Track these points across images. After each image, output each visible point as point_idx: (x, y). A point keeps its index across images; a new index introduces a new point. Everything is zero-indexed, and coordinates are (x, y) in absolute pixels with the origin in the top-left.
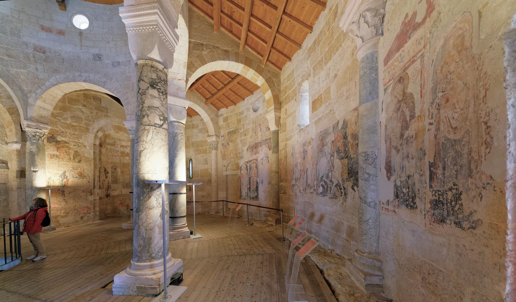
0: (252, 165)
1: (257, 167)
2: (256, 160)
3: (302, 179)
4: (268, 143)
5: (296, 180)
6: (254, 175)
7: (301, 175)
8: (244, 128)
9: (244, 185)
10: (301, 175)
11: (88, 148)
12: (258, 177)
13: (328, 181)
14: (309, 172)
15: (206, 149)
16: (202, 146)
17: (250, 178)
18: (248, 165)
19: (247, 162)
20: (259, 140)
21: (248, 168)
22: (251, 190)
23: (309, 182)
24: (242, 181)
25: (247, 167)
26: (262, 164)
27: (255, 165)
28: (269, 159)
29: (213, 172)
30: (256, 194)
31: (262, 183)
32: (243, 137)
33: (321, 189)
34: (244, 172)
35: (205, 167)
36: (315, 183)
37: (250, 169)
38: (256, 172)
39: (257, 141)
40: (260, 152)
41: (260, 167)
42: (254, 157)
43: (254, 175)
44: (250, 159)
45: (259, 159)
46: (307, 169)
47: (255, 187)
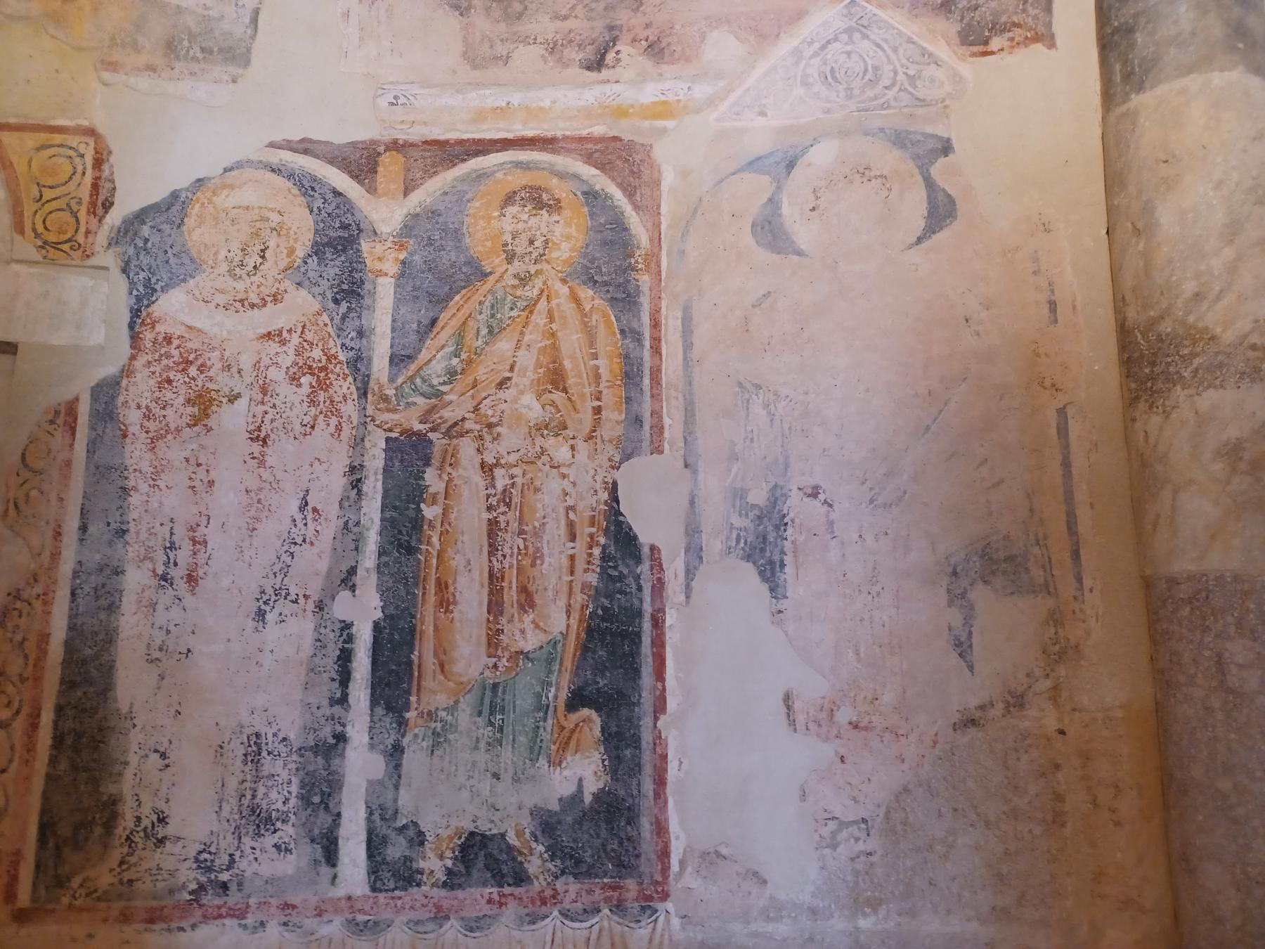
0: (489, 228)
1: (614, 270)
2: (619, 156)
6: (531, 407)
9: (234, 568)
17: (410, 453)
18: (384, 213)
19: (362, 162)
21: (382, 262)
22: (433, 694)
24: (157, 503)
25: (340, 239)
26: (771, 232)
27: (566, 235)
30: (584, 772)
31: (765, 551)
37: (443, 277)
38: (589, 349)
40: (722, 48)
41: (708, 288)
42: (569, 101)
43: (531, 407)
44: (451, 111)
45: (677, 159)
47: (556, 619)
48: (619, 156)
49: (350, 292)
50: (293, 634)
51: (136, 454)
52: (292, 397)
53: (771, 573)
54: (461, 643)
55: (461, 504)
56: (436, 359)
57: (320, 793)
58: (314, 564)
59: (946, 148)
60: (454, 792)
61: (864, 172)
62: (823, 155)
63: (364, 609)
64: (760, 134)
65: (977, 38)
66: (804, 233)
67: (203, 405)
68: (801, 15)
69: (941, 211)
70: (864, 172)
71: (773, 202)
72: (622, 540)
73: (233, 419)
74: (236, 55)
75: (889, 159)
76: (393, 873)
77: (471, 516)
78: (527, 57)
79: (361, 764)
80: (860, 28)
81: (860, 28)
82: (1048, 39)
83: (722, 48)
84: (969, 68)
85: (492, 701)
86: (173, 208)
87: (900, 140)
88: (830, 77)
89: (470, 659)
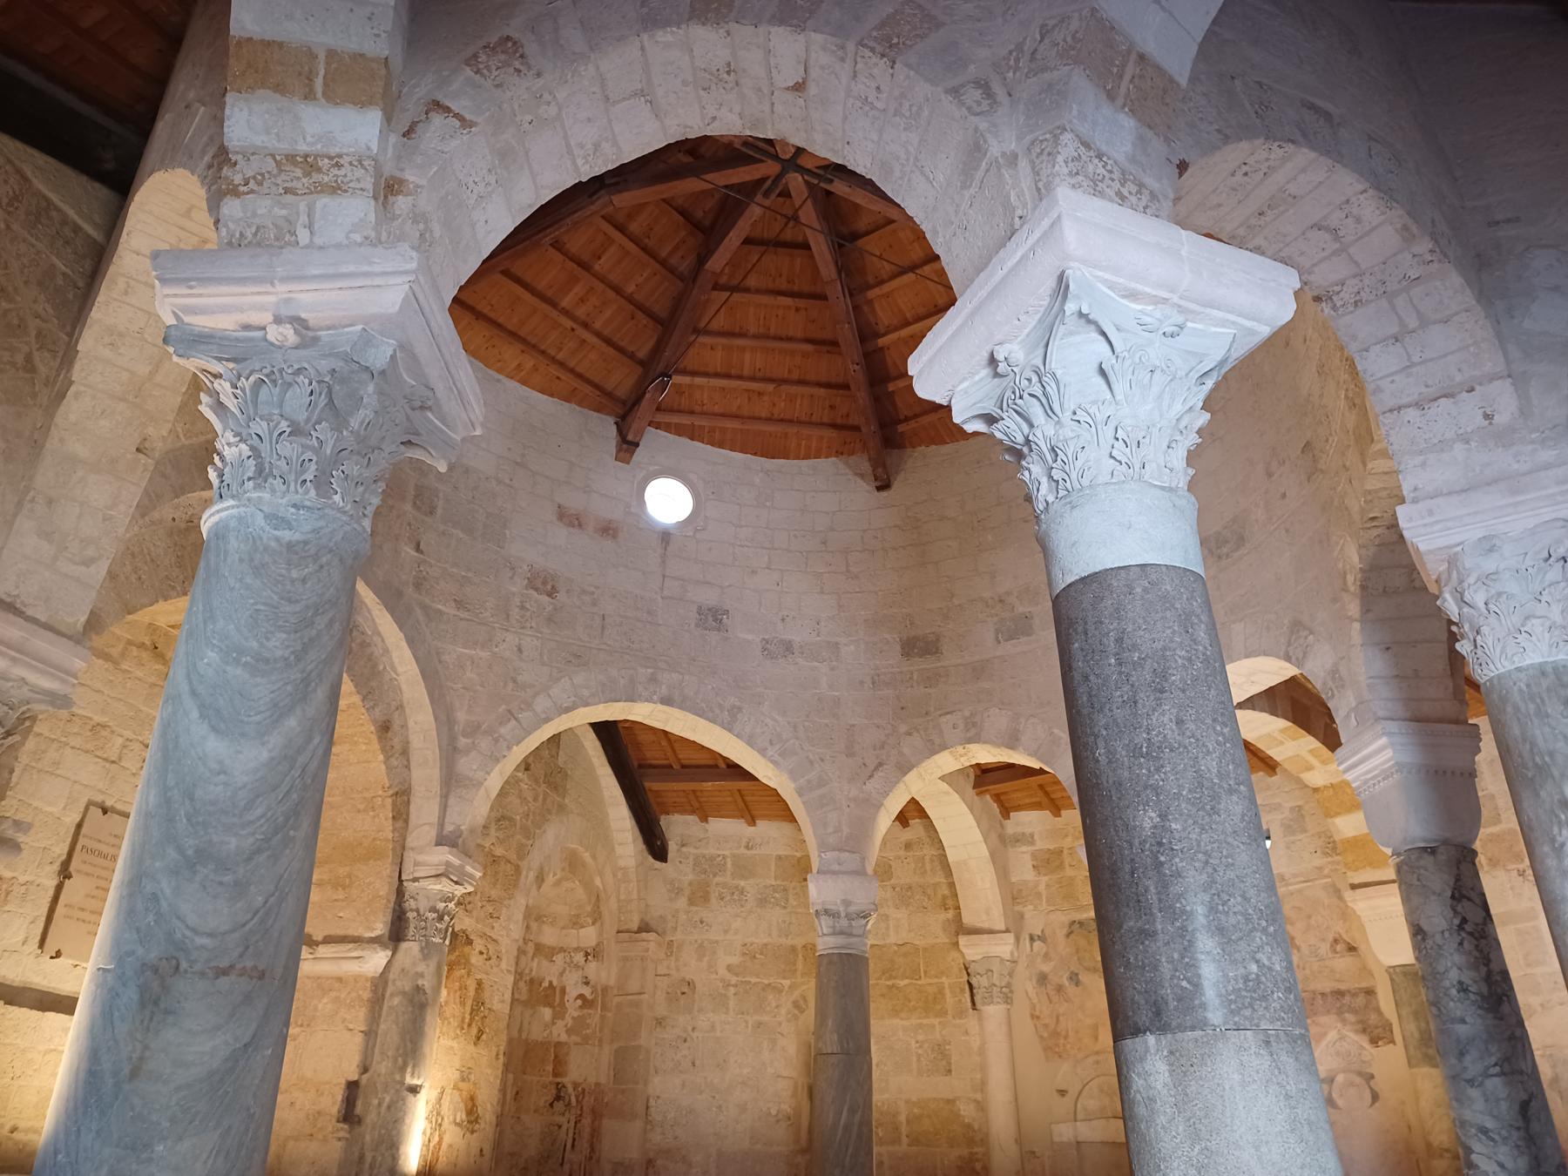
4: (1354, 1011)
11: (504, 965)
15: (941, 991)
16: (915, 974)
28: (1379, 1084)
29: (1001, 1124)
35: (936, 1088)
59: (1372, 1077)
61: (1352, 1084)
62: (1340, 1078)
65: (1374, 1041)
66: (1340, 1102)
68: (1325, 1034)
69: (1375, 1097)
70: (1352, 1084)
71: (1330, 1093)
75: (1358, 1080)
80: (1342, 1038)
81: (1342, 1038)
82: (1393, 1042)
84: (1374, 1051)
87: (1360, 1074)
88: (1338, 1054)
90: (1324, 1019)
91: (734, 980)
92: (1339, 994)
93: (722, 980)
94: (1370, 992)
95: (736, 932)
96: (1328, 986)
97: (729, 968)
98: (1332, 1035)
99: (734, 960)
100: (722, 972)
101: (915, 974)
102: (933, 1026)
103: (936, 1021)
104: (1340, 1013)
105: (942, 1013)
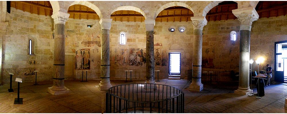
0: (85, 52)
1: (89, 53)
3: (121, 60)
5: (118, 61)
7: (120, 59)
8: (79, 31)
9: (79, 61)
10: (120, 59)
12: (90, 58)
13: (134, 62)
14: (125, 59)
18: (83, 51)
19: (82, 50)
20: (92, 40)
21: (83, 53)
22: (84, 64)
23: (125, 61)
24: (77, 59)
25: (81, 52)
26: (93, 52)
27: (88, 52)
30: (88, 66)
32: (78, 36)
33: (131, 64)
34: (79, 54)
36: (128, 62)
39: (90, 40)
40: (92, 46)
41: (91, 53)
42: (88, 48)
44: (84, 48)
45: (91, 50)
46: (124, 58)
47: (87, 63)
48: (89, 49)
49: (82, 54)
50: (81, 63)
51: (77, 58)
52: (80, 57)
53: (93, 61)
54: (85, 63)
55: (85, 59)
56: (84, 55)
57: (82, 67)
58: (81, 61)
60: (85, 67)
62: (95, 50)
63: (82, 62)
64: (93, 49)
65: (99, 47)
67: (78, 57)
72: (89, 61)
73: (79, 57)
74: (78, 47)
76: (83, 69)
77: (85, 60)
78: (87, 46)
79: (83, 66)
83: (92, 46)
85: (86, 65)
86: (77, 51)
89: (85, 63)
90: (94, 44)
91: (20, 31)
92: (97, 42)
93: (18, 31)
94: (100, 42)
95: (20, 25)
96: (96, 41)
97: (19, 29)
98: (95, 46)
99: (20, 29)
100: (18, 30)
101: (46, 34)
102: (48, 40)
103: (48, 39)
104: (96, 44)
105: (49, 38)
